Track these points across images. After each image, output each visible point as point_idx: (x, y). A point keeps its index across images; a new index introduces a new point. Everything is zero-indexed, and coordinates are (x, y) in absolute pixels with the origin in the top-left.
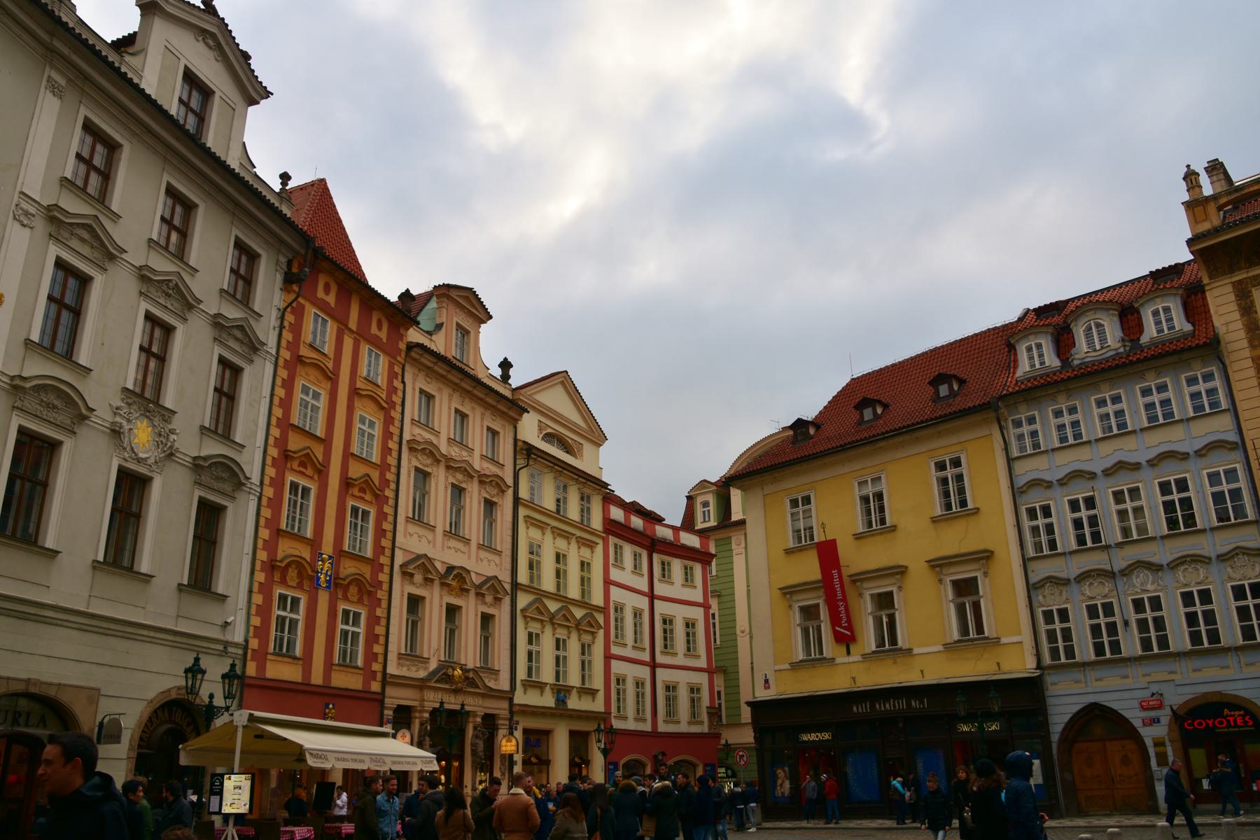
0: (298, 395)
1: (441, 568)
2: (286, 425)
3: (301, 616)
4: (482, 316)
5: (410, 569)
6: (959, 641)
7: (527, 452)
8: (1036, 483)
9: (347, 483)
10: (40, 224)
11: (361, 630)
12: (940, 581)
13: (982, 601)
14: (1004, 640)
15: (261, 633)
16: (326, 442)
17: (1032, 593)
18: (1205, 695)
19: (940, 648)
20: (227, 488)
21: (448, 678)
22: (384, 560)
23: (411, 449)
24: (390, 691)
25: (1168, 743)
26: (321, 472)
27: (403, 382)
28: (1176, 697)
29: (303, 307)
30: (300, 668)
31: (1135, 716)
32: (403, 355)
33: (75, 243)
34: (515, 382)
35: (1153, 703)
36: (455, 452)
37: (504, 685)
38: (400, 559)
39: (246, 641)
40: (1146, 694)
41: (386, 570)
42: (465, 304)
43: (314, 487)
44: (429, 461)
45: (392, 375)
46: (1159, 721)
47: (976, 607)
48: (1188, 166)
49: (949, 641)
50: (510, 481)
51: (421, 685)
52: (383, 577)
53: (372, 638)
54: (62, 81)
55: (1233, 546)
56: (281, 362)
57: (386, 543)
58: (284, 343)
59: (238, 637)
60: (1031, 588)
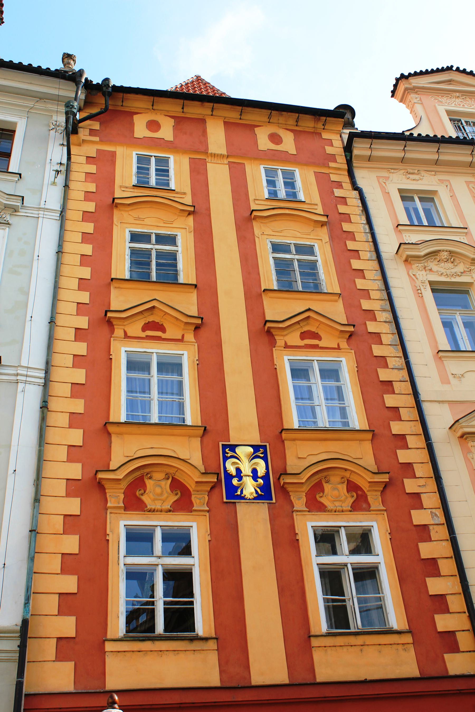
2: (100, 283)
9: (265, 334)
15: (87, 603)
22: (405, 426)
23: (408, 261)
29: (113, 154)
30: (213, 658)
32: (342, 160)
39: (25, 623)
43: (187, 357)
44: (461, 268)
45: (326, 186)
52: (413, 454)
56: (74, 215)
57: (399, 399)
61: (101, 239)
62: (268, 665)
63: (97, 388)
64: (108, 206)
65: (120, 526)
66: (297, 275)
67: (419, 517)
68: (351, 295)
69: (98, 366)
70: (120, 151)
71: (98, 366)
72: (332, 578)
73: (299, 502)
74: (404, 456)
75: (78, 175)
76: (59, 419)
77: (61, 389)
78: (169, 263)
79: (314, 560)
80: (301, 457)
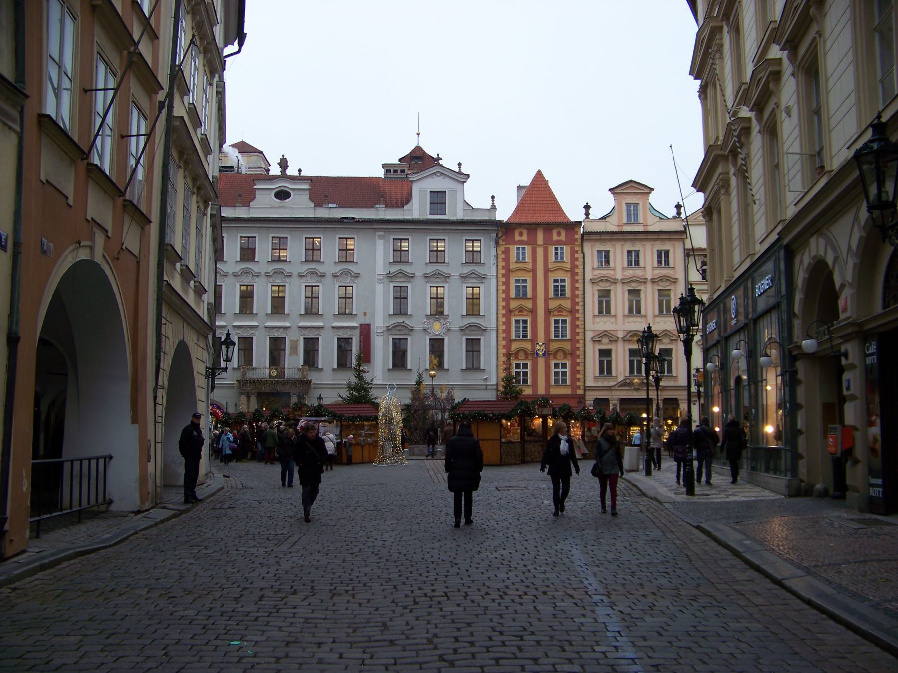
0: (513, 285)
1: (620, 335)
2: (507, 299)
3: (529, 370)
4: (646, 191)
5: (596, 339)
7: (690, 253)
9: (548, 312)
10: (386, 280)
11: (568, 370)
16: (534, 299)
20: (480, 332)
21: (631, 384)
24: (587, 393)
26: (533, 311)
27: (583, 253)
32: (579, 241)
33: (398, 280)
34: (683, 216)
36: (629, 273)
37: (683, 382)
38: (589, 335)
41: (581, 342)
42: (631, 191)
43: (529, 320)
44: (608, 284)
50: (681, 275)
51: (610, 389)
52: (580, 345)
53: (574, 372)
54: (382, 233)
56: (500, 275)
58: (500, 267)
59: (494, 383)
61: (507, 283)
62: (541, 391)
63: (508, 331)
64: (508, 272)
65: (514, 363)
66: (560, 292)
67: (578, 361)
68: (574, 296)
69: (508, 323)
70: (511, 247)
71: (508, 323)
72: (556, 374)
73: (551, 357)
74: (578, 345)
75: (500, 260)
76: (500, 339)
77: (500, 331)
78: (525, 293)
79: (553, 370)
80: (554, 346)
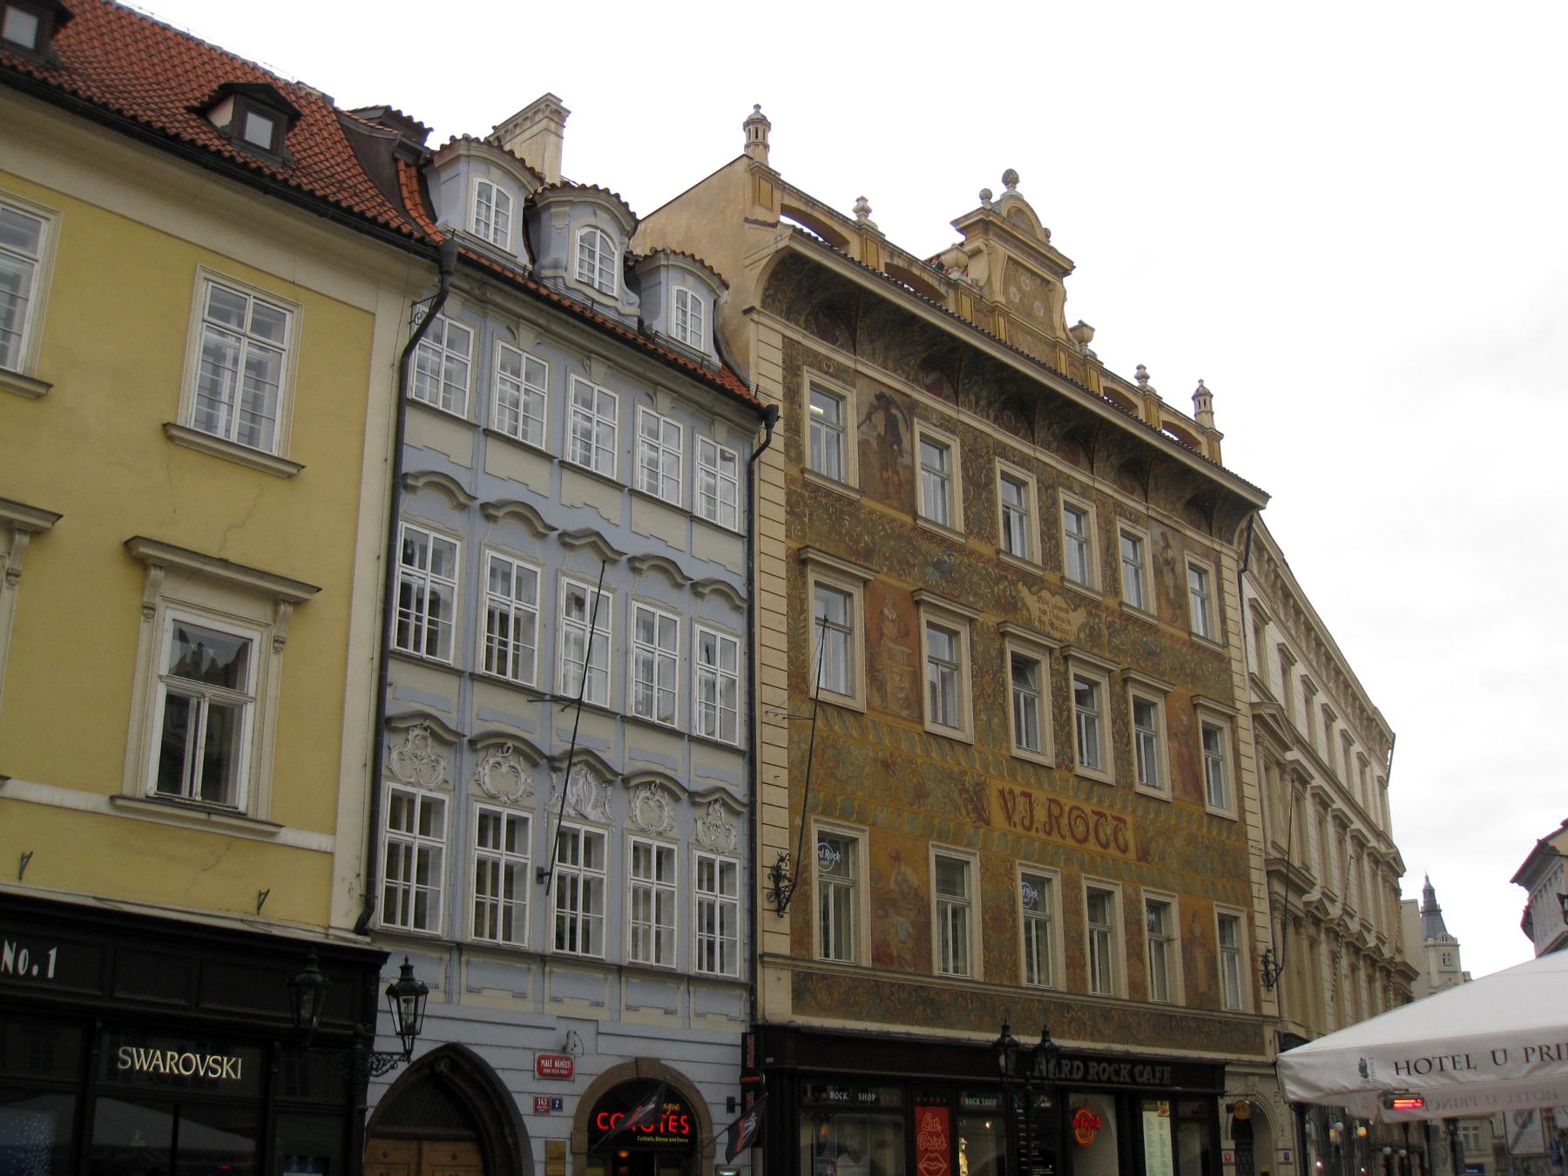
6: (148, 799)
8: (445, 485)
12: (149, 610)
13: (249, 715)
14: (287, 836)
17: (389, 739)
18: (637, 1061)
19: (99, 802)
25: (569, 1158)
28: (597, 1061)
31: (522, 1087)
35: (554, 1066)
40: (547, 1041)
46: (561, 1106)
47: (224, 721)
48: (757, 107)
49: (127, 791)
55: (711, 783)
60: (383, 724)
